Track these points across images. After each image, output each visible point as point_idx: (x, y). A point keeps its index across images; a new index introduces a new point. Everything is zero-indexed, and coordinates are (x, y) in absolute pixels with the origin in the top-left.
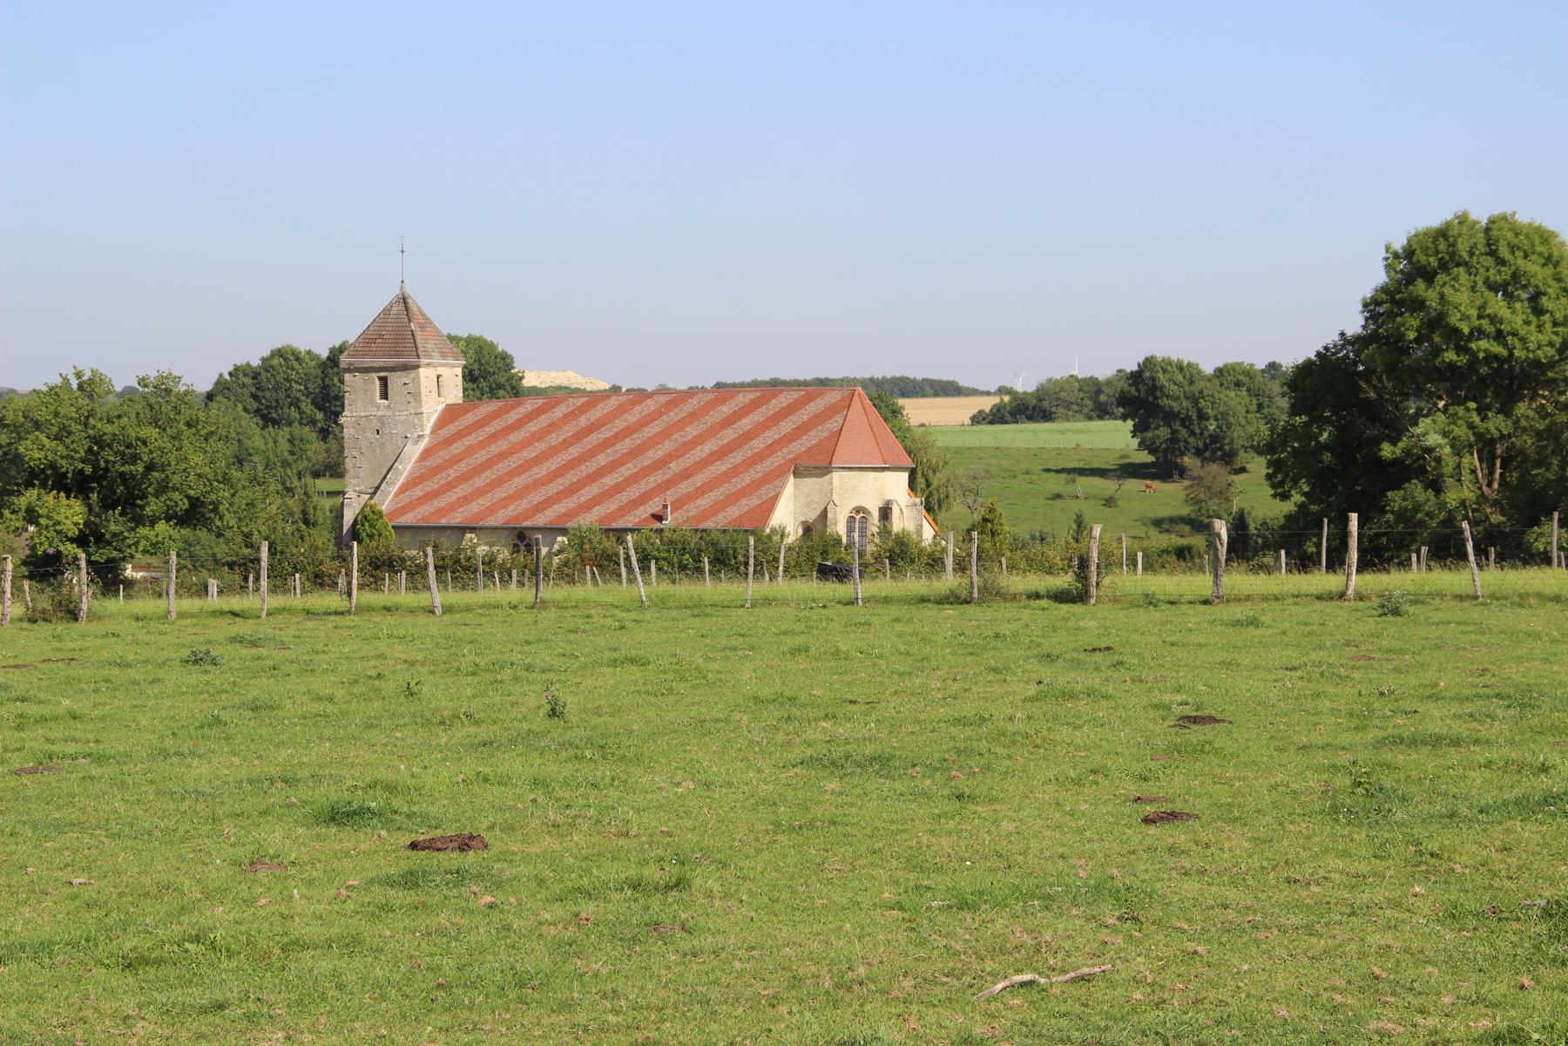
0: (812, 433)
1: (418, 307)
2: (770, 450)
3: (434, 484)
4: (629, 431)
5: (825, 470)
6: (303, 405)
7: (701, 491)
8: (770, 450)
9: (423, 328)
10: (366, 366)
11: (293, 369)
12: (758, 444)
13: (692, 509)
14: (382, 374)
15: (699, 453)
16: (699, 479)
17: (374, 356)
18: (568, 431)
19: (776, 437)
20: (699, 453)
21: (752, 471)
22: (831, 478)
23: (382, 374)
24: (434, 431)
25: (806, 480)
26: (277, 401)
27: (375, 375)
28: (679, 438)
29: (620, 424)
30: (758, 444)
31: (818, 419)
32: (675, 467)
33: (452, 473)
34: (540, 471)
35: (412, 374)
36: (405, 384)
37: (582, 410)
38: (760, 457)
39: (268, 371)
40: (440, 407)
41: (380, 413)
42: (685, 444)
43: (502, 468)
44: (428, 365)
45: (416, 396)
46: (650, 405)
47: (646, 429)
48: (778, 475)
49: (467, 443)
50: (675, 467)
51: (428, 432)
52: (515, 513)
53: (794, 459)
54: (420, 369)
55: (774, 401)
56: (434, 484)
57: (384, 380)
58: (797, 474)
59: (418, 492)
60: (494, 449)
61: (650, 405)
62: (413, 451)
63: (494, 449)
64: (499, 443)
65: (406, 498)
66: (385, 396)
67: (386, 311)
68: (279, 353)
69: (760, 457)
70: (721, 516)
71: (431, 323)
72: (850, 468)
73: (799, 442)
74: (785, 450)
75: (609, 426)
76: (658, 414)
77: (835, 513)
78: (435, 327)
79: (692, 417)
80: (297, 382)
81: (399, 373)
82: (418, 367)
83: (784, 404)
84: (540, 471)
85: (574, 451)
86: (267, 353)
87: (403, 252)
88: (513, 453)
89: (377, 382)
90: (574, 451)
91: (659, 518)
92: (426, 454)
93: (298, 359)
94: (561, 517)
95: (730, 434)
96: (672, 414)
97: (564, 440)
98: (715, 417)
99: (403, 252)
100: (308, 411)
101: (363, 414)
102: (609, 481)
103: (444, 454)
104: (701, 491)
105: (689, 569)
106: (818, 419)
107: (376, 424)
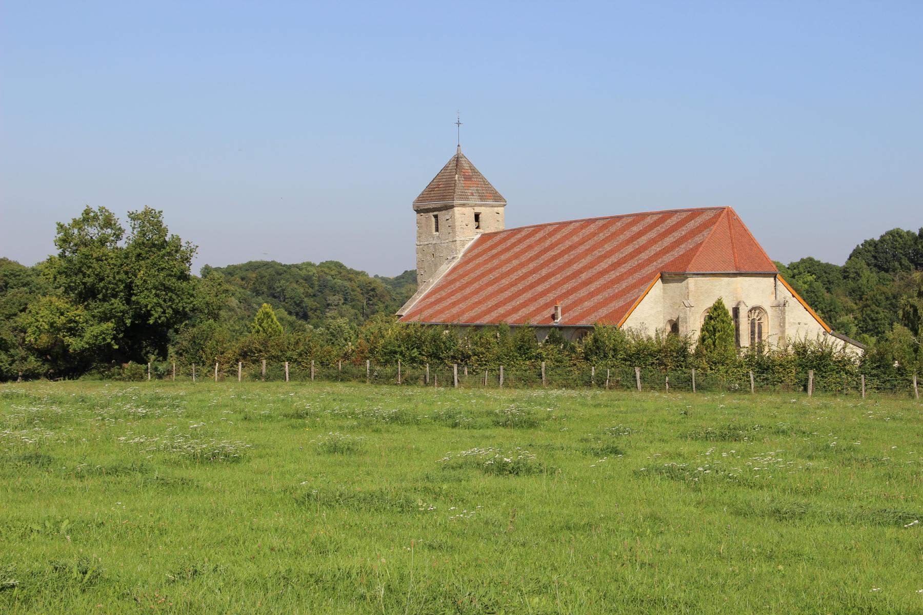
0: (683, 246)
1: (469, 163)
2: (650, 261)
3: (443, 293)
4: (572, 248)
5: (681, 277)
6: (903, 262)
7: (591, 295)
8: (650, 261)
9: (468, 178)
10: (426, 207)
11: (897, 241)
12: (644, 256)
13: (577, 311)
14: (435, 213)
15: (604, 265)
16: (592, 287)
17: (431, 200)
18: (537, 249)
19: (658, 249)
20: (604, 265)
21: (630, 278)
22: (688, 283)
23: (435, 213)
24: (464, 256)
25: (671, 284)
26: (886, 258)
27: (431, 214)
28: (597, 253)
29: (568, 243)
30: (644, 256)
31: (693, 233)
32: (584, 276)
33: (458, 284)
34: (505, 282)
35: (450, 212)
36: (447, 220)
37: (551, 234)
38: (640, 267)
39: (882, 243)
40: (479, 236)
41: (434, 242)
42: (600, 257)
43: (486, 280)
44: (463, 205)
45: (452, 227)
46: (592, 228)
47: (581, 247)
48: (647, 281)
49: (477, 262)
50: (584, 276)
51: (460, 255)
52: (475, 314)
53: (662, 268)
54: (455, 208)
55: (669, 221)
56: (443, 293)
57: (436, 217)
58: (664, 280)
59: (433, 299)
60: (489, 266)
61: (592, 228)
62: (445, 269)
63: (489, 266)
64: (494, 261)
65: (424, 304)
66: (437, 230)
67: (446, 168)
68: (890, 233)
69: (640, 267)
70: (593, 316)
71: (480, 174)
72: (698, 274)
73: (672, 253)
74: (659, 261)
75: (561, 245)
76: (594, 234)
77: (685, 313)
78: (483, 178)
79: (614, 235)
80: (900, 249)
81: (444, 212)
82: (452, 207)
83: (674, 223)
84: (505, 282)
85: (531, 266)
86: (883, 233)
87: (459, 124)
88: (497, 268)
89: (433, 219)
90: (531, 266)
91: (554, 317)
92: (455, 269)
93: (900, 236)
94: (499, 316)
95: (630, 249)
96: (601, 234)
97: (530, 258)
98: (628, 234)
99: (459, 124)
100: (906, 264)
101: (426, 243)
102: (540, 288)
103: (461, 271)
104: (591, 295)
105: (416, 362)
106: (693, 233)
107: (432, 250)
